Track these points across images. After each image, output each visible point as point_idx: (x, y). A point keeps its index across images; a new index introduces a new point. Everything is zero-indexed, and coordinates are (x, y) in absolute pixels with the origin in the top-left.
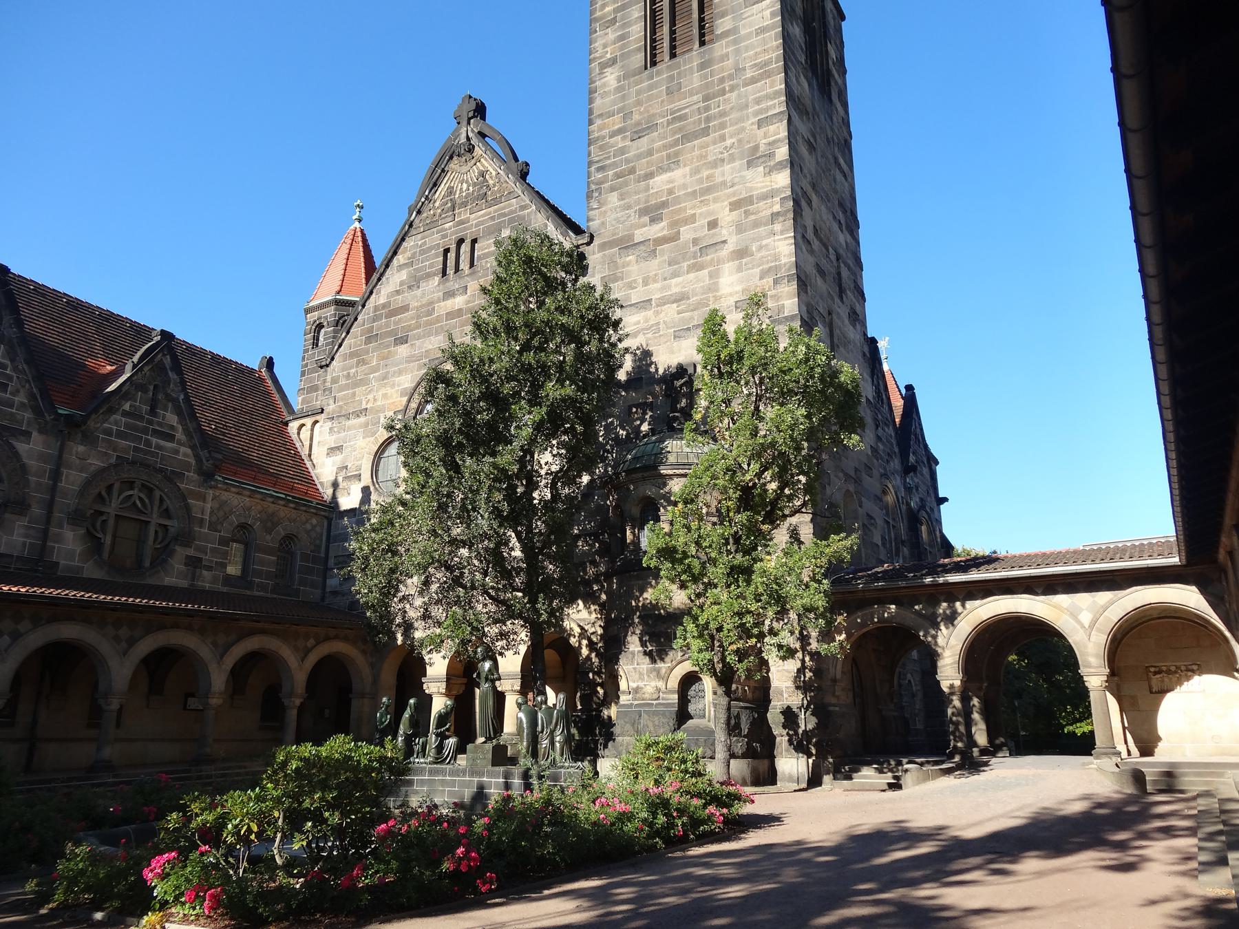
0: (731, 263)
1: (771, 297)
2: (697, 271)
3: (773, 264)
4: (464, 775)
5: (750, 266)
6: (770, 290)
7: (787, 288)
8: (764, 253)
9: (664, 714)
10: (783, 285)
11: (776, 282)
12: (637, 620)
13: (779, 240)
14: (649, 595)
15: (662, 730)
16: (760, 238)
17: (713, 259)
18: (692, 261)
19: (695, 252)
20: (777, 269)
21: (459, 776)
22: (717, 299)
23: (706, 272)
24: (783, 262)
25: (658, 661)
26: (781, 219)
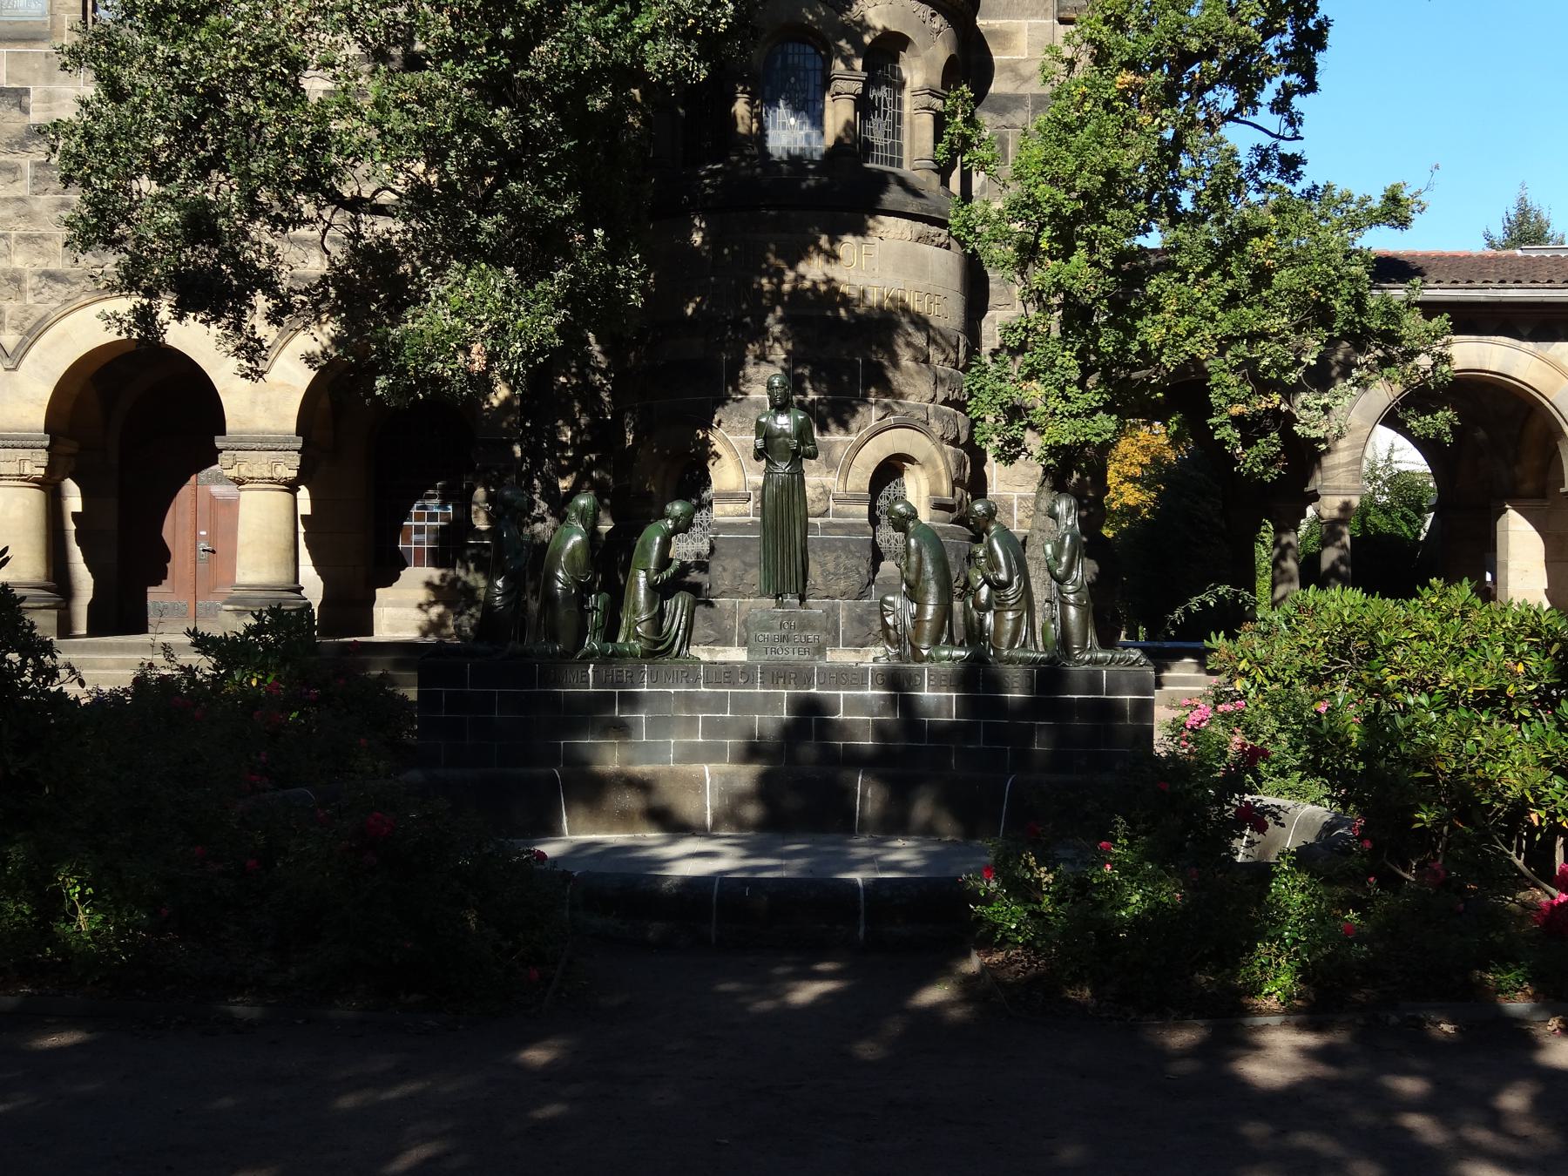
4: (750, 682)
9: (845, 545)
12: (777, 329)
14: (814, 269)
15: (842, 585)
21: (733, 684)
25: (833, 427)
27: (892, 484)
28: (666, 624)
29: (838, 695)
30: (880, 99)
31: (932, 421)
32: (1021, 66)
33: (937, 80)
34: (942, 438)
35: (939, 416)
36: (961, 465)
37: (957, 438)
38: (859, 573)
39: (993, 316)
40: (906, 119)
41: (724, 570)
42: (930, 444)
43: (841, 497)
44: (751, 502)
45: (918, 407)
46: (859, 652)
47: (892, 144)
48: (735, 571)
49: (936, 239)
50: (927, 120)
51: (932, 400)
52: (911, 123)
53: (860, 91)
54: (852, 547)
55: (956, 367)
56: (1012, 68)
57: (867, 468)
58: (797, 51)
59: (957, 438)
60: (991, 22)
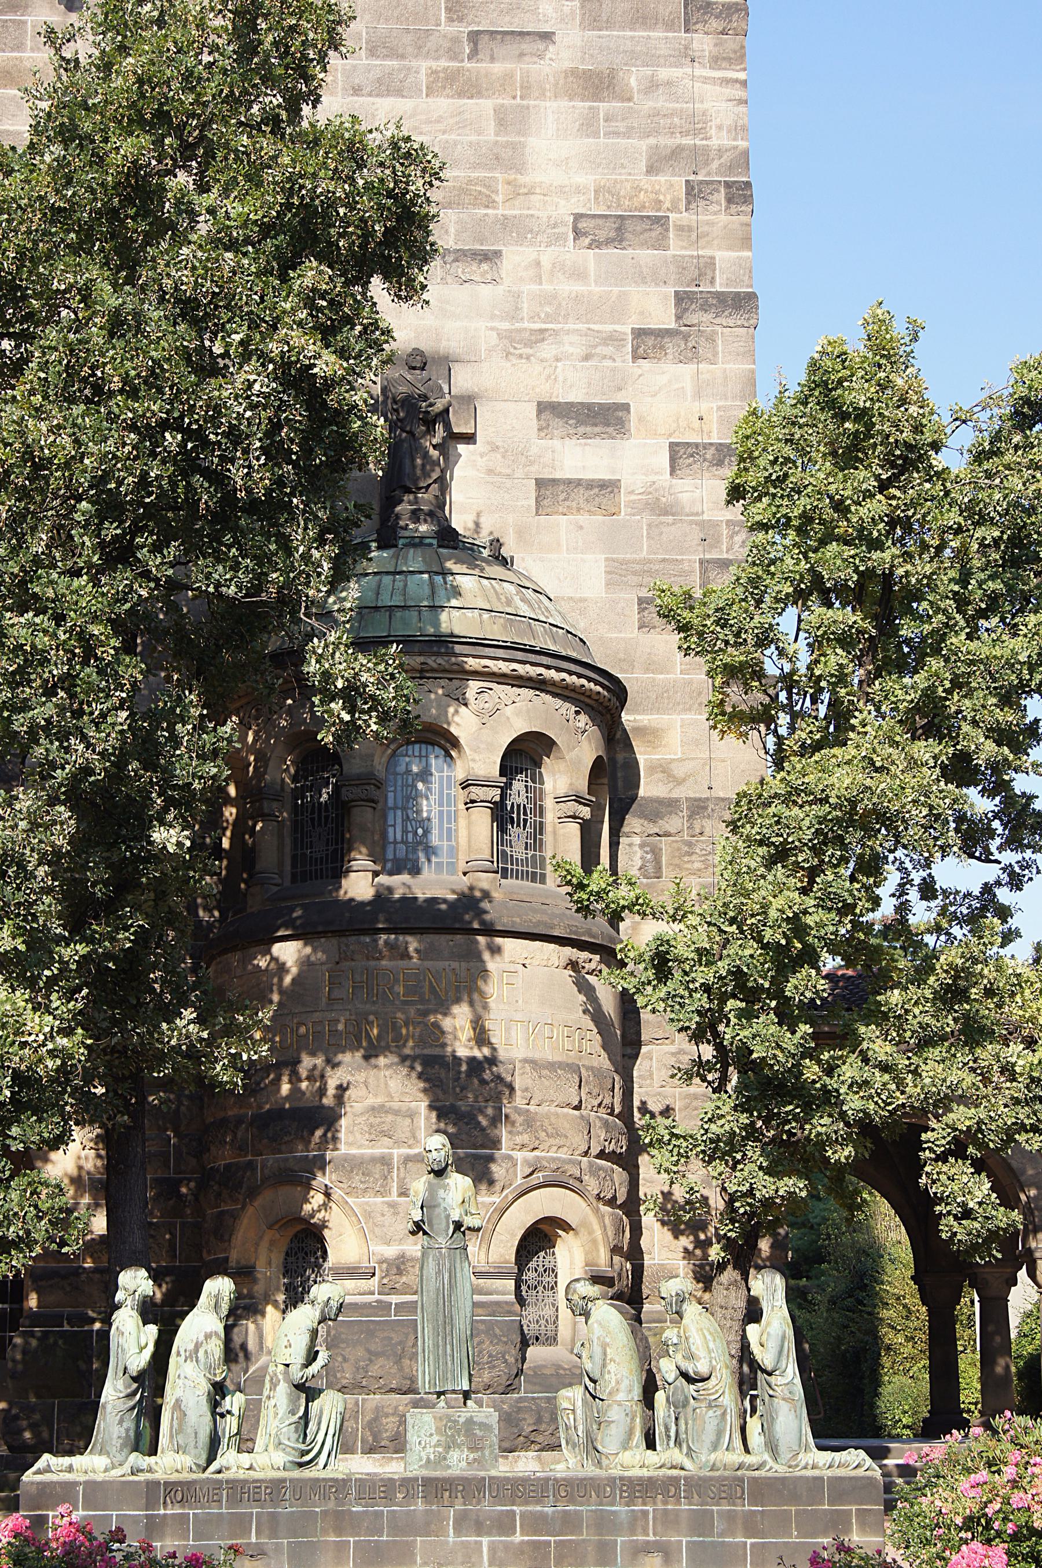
0: (564, 103)
1: (680, 228)
2: (460, 94)
3: (687, 141)
5: (621, 126)
6: (674, 208)
7: (723, 218)
8: (660, 102)
10: (715, 208)
11: (694, 193)
13: (705, 80)
15: (486, 1376)
16: (651, 59)
17: (509, 76)
18: (444, 63)
19: (456, 40)
20: (699, 156)
22: (517, 192)
23: (486, 105)
24: (714, 142)
26: (715, 24)
27: (542, 1254)
28: (312, 1427)
29: (513, 1512)
30: (519, 806)
31: (586, 1178)
32: (673, 766)
33: (582, 785)
34: (598, 1197)
35: (594, 1171)
36: (620, 1230)
37: (614, 1198)
38: (506, 1361)
39: (650, 1052)
40: (548, 829)
41: (345, 1360)
42: (584, 1204)
43: (483, 1270)
44: (376, 1278)
45: (570, 1161)
46: (507, 1457)
47: (534, 856)
48: (357, 1361)
49: (587, 965)
50: (574, 829)
51: (586, 1154)
52: (555, 833)
53: (497, 798)
54: (497, 1331)
55: (611, 1114)
56: (664, 769)
57: (513, 1235)
58: (424, 753)
59: (614, 1198)
60: (638, 717)
